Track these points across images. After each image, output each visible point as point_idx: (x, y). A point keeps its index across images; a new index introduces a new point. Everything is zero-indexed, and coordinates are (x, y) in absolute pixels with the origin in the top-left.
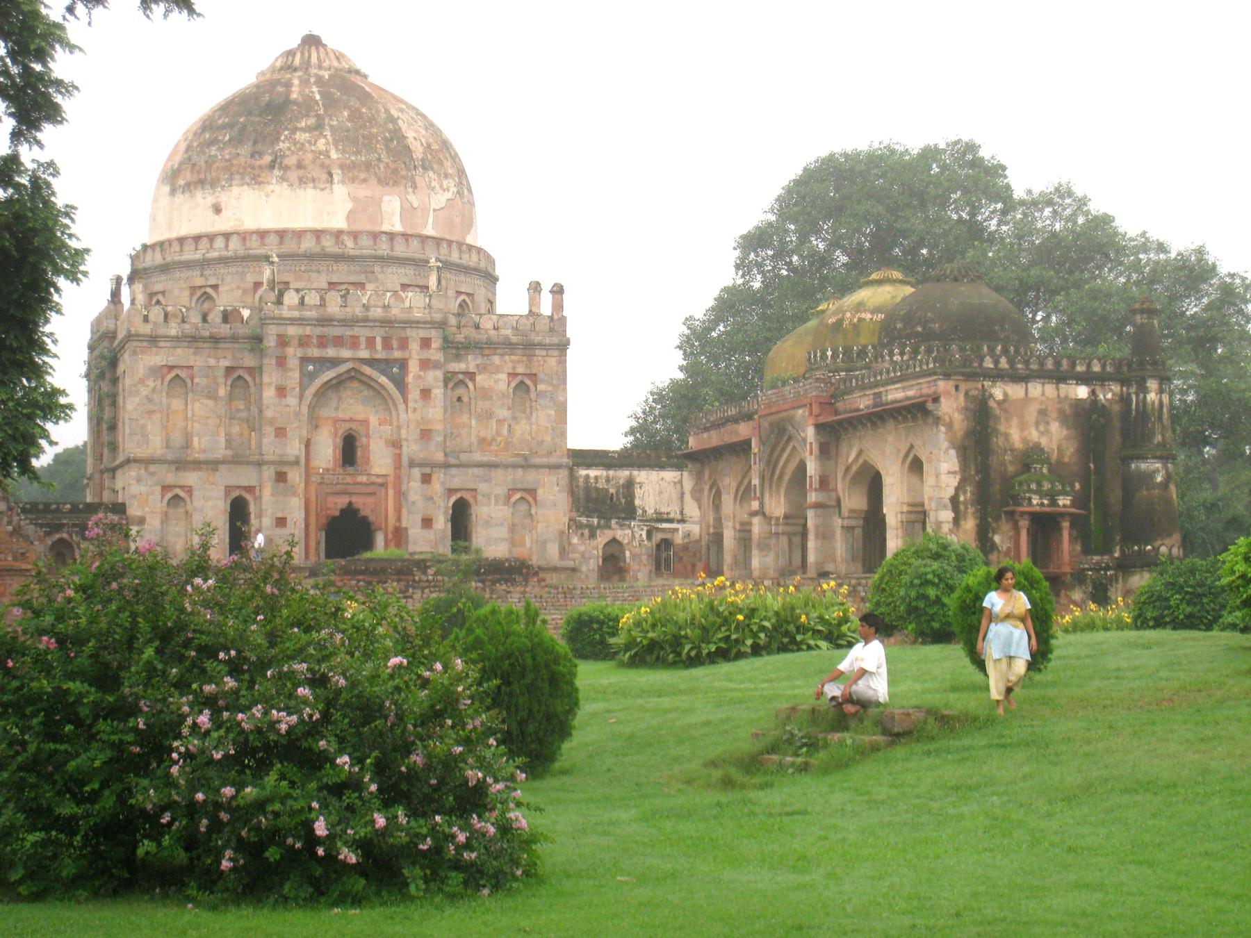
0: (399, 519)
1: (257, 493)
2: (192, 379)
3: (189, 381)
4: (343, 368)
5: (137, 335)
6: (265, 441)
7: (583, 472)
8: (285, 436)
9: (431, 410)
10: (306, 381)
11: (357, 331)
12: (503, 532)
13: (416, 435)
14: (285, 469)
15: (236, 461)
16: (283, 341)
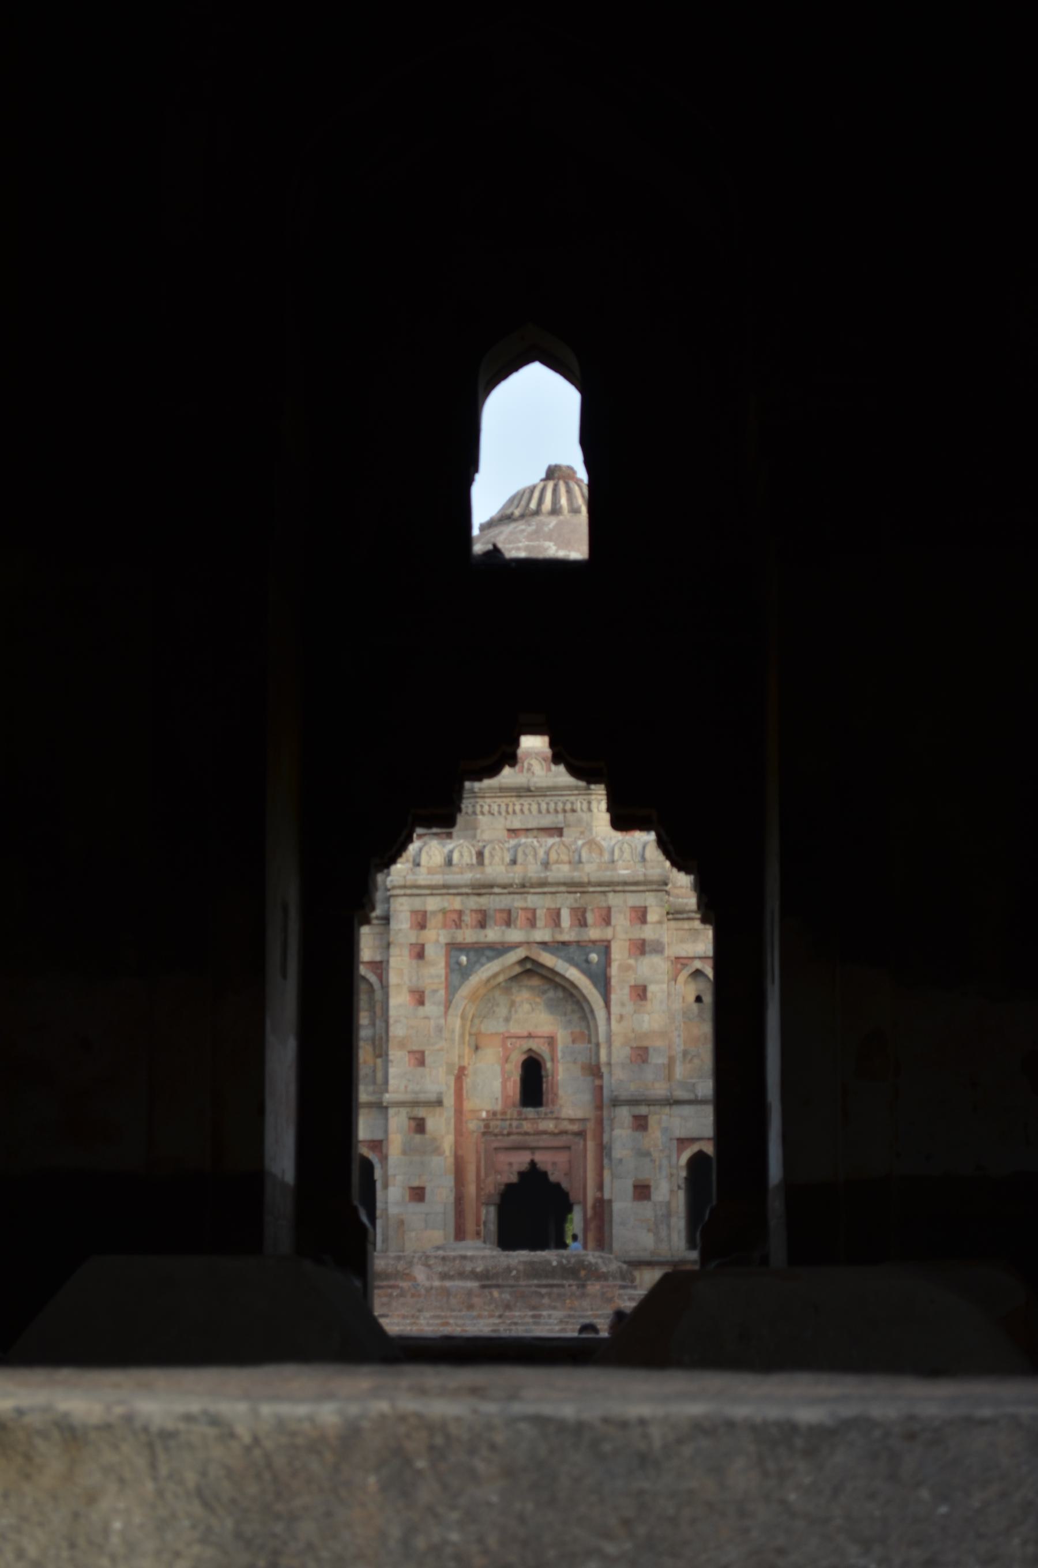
0: (600, 1187)
1: (384, 1151)
6: (392, 1071)
9: (646, 1017)
10: (455, 978)
11: (532, 900)
14: (421, 1112)
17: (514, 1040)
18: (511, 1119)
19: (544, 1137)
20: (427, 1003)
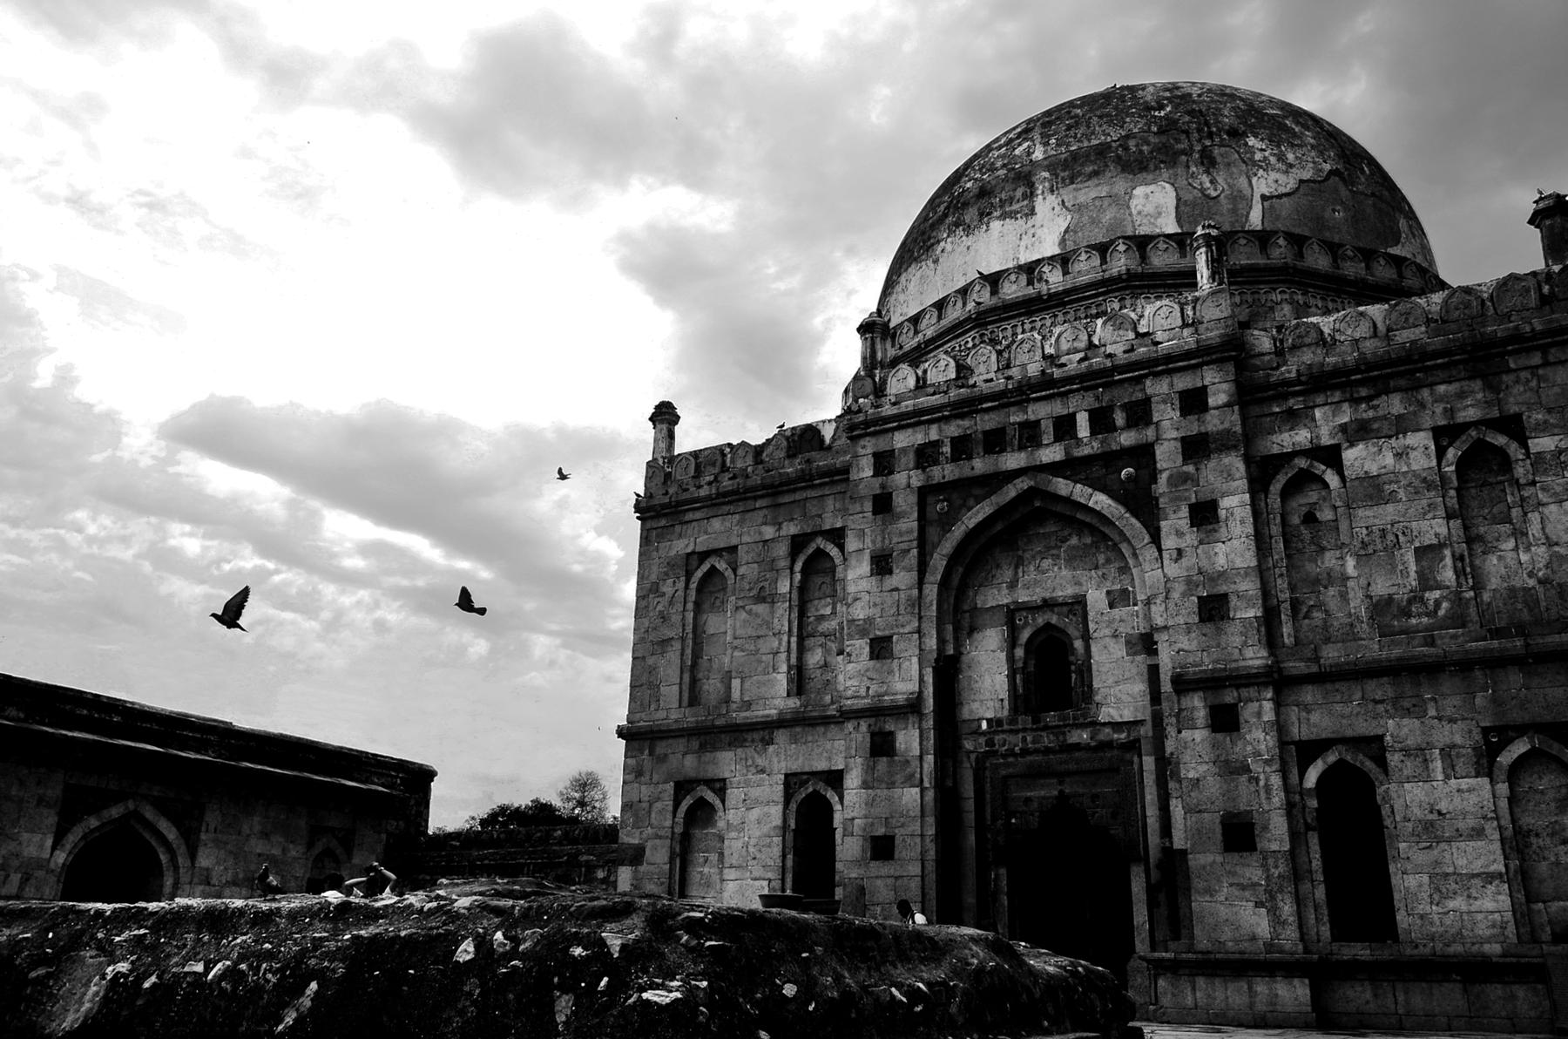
2: (735, 570)
3: (729, 573)
4: (1011, 492)
8: (891, 656)
9: (1220, 548)
12: (1486, 855)
13: (1188, 611)
14: (890, 727)
18: (1024, 730)
20: (896, 571)
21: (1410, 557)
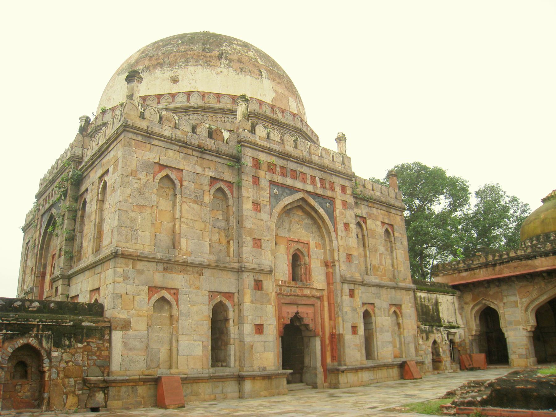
1: (236, 300)
2: (181, 181)
4: (298, 196)
5: (132, 127)
6: (245, 249)
7: (419, 294)
9: (350, 239)
10: (273, 200)
11: (305, 169)
13: (343, 258)
15: (218, 267)
16: (257, 164)
17: (291, 242)
19: (304, 298)
21: (378, 255)
